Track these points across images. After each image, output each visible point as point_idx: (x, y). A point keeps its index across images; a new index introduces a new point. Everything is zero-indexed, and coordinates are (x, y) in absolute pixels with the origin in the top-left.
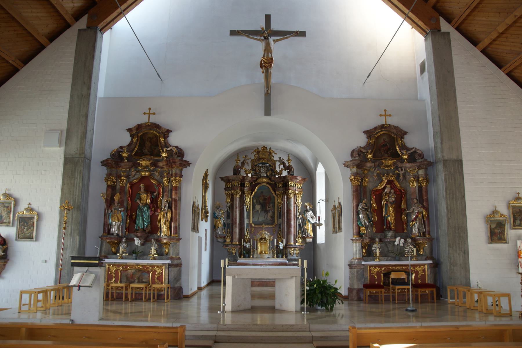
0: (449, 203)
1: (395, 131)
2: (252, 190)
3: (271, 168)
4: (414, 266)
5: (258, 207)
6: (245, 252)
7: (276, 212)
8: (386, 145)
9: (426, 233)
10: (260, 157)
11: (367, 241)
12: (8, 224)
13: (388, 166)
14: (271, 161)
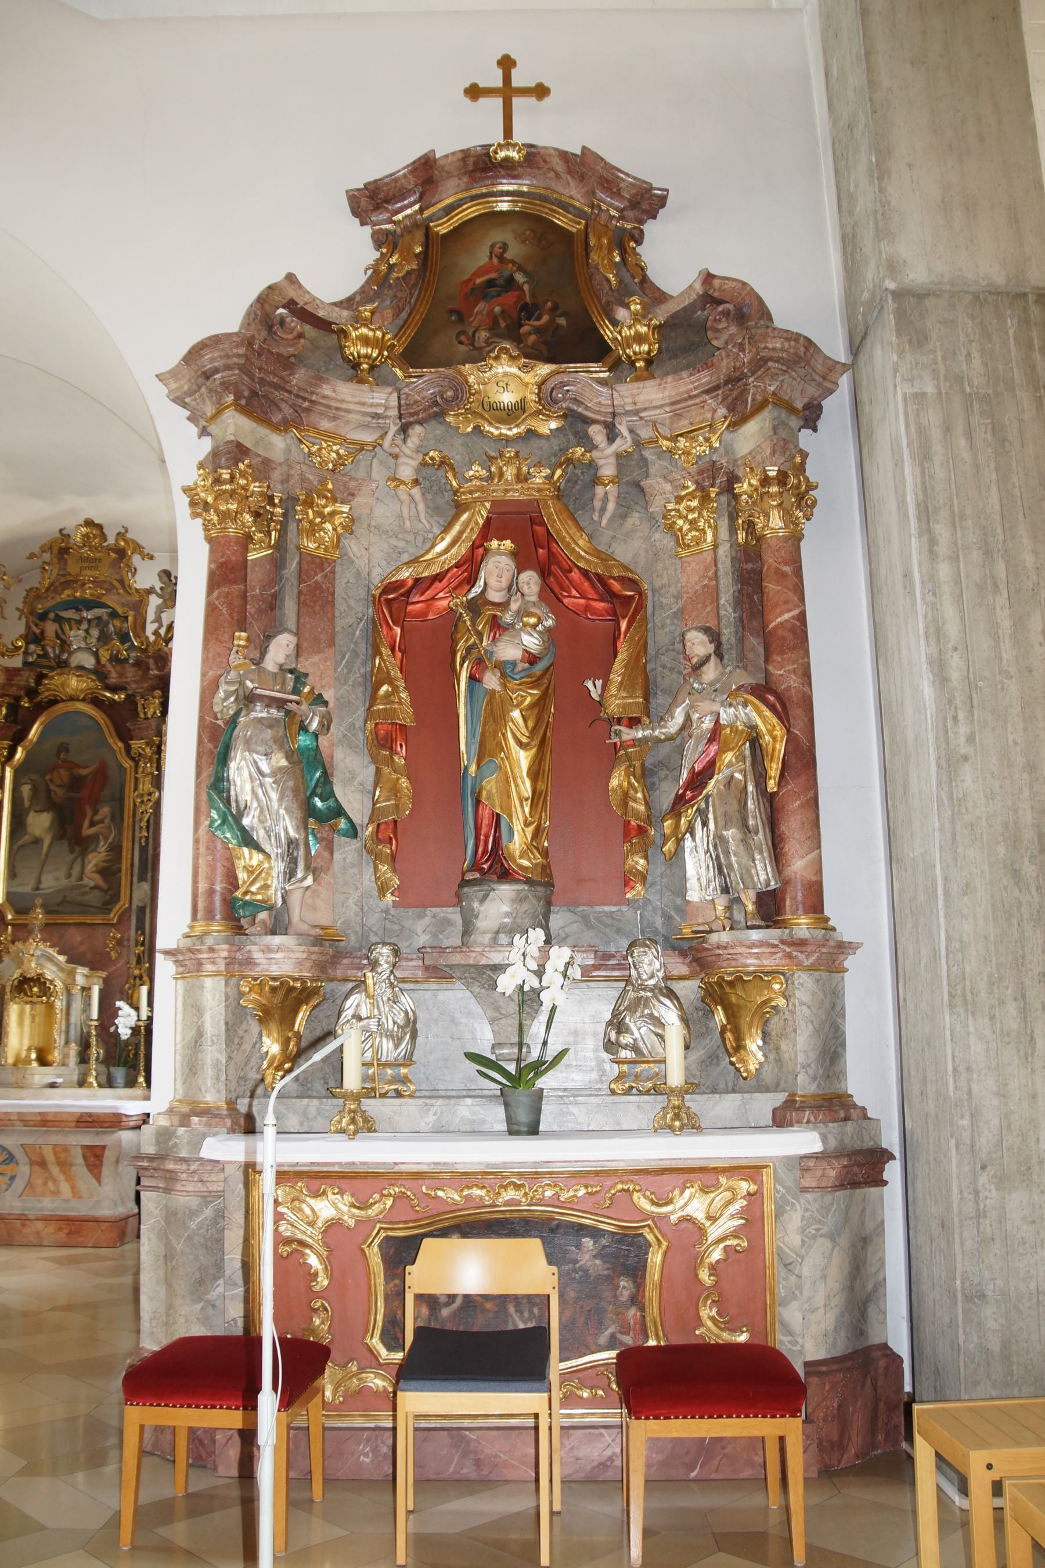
0: (952, 629)
3: (117, 623)
5: (40, 823)
7: (126, 845)
8: (510, 282)
10: (69, 574)
14: (121, 591)
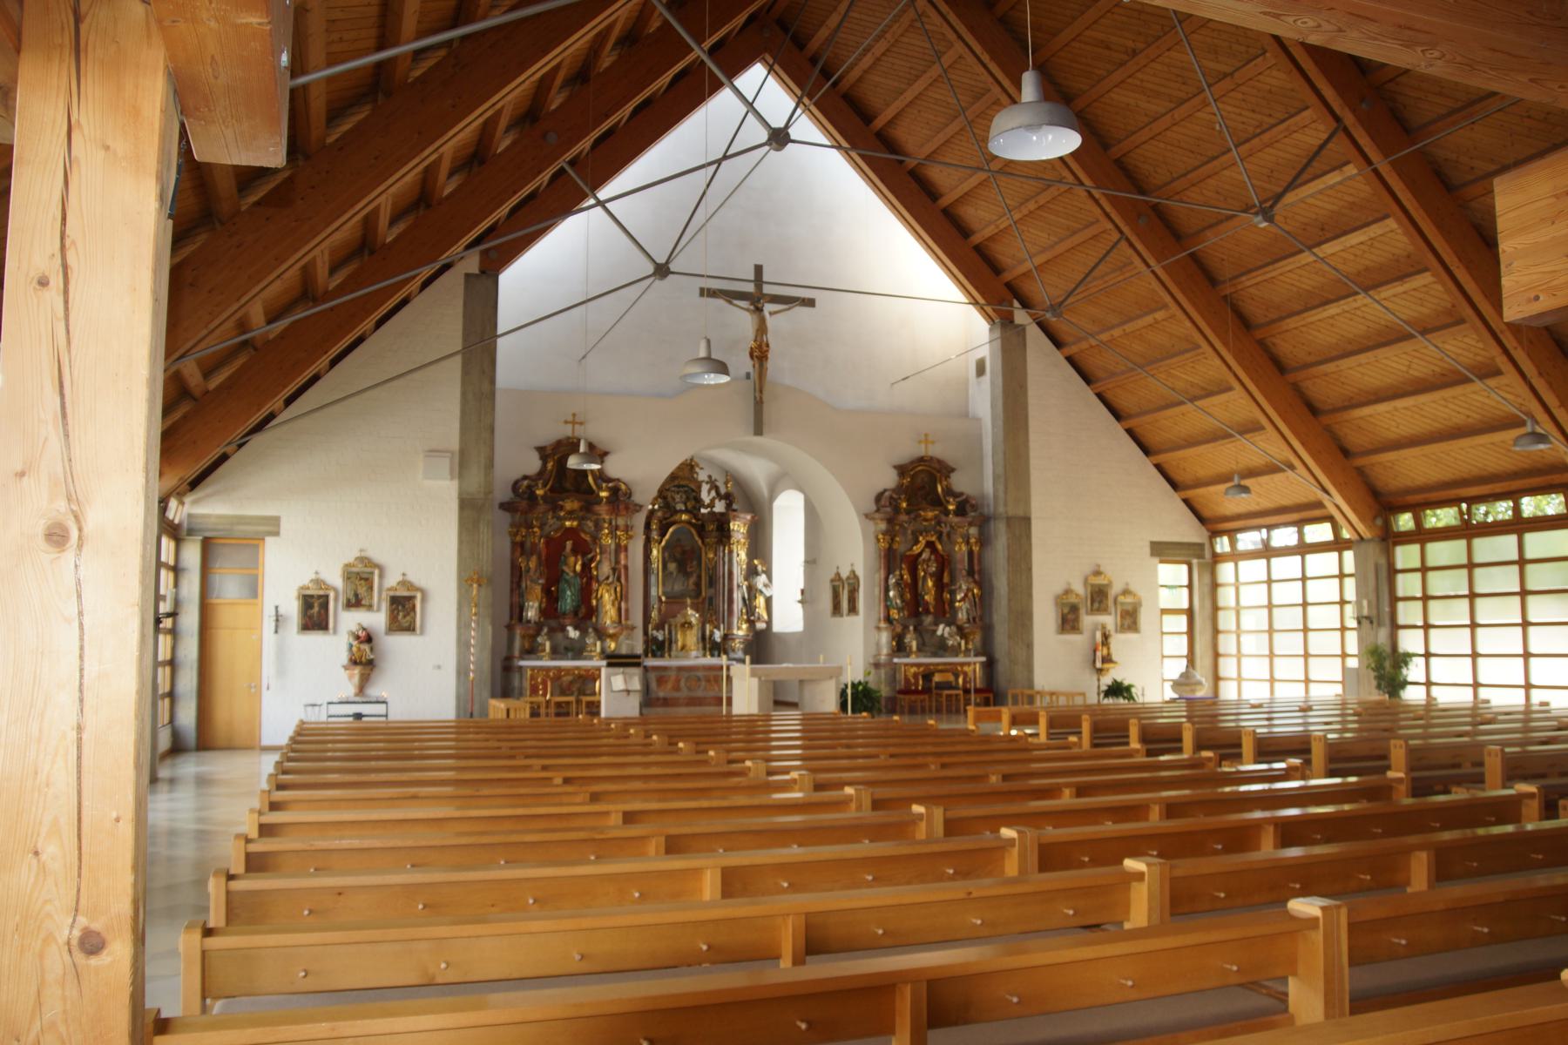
1: (937, 466)
2: (663, 535)
3: (694, 494)
4: (963, 664)
5: (672, 566)
6: (654, 648)
9: (977, 620)
11: (899, 629)
12: (370, 607)
13: (926, 520)
